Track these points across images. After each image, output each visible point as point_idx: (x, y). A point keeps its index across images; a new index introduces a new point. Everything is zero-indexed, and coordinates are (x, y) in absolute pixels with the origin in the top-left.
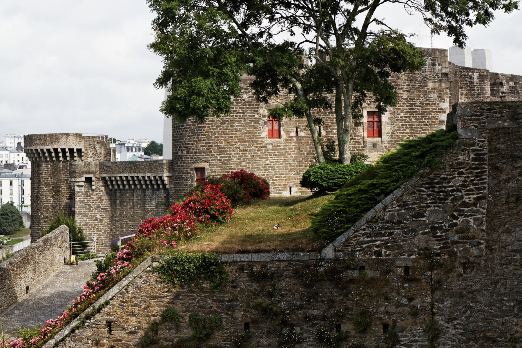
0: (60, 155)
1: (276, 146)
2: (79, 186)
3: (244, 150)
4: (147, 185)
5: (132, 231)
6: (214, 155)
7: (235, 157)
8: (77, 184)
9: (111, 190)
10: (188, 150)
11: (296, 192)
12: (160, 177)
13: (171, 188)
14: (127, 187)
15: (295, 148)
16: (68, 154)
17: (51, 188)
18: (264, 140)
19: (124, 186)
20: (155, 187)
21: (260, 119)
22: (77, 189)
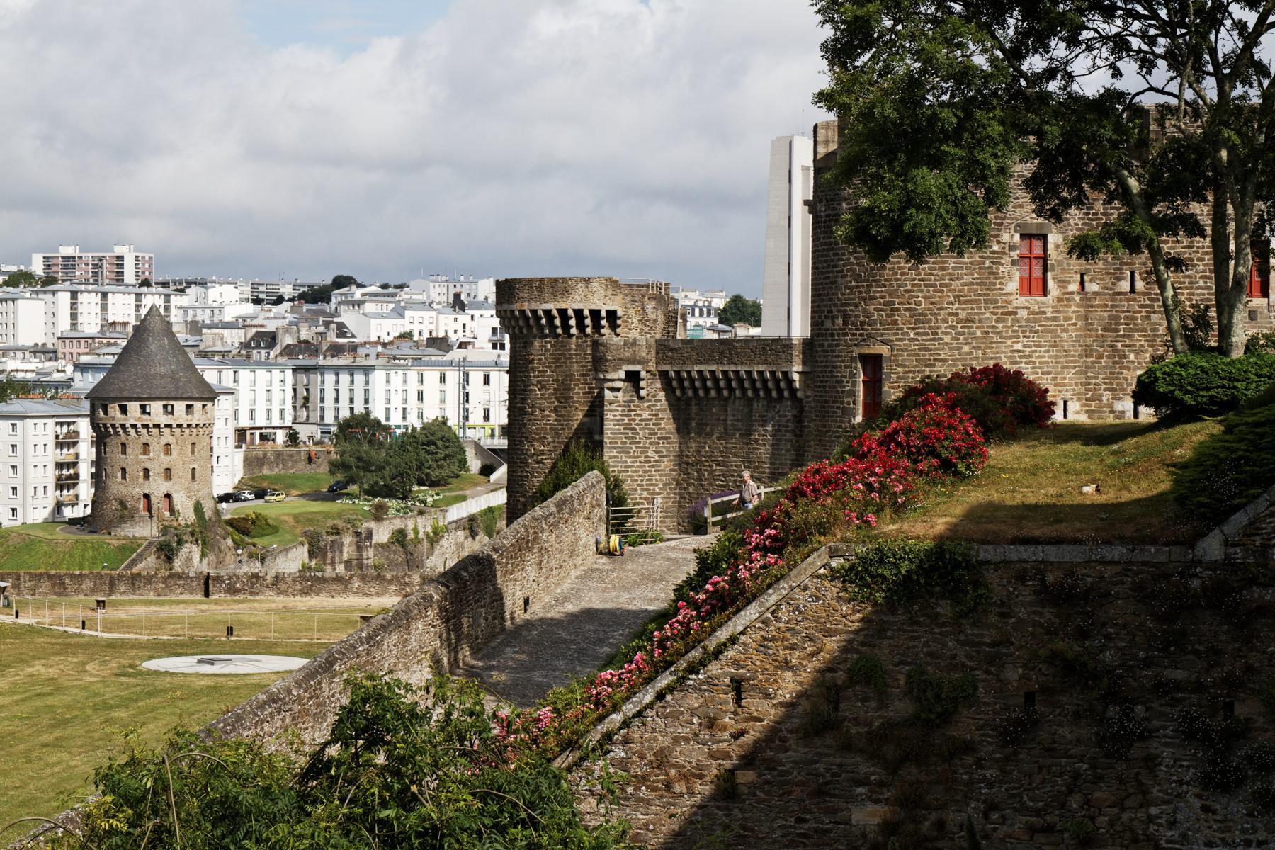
0: (573, 322)
1: (1038, 313)
2: (613, 389)
3: (967, 320)
4: (756, 391)
6: (902, 329)
7: (947, 334)
8: (609, 384)
9: (679, 399)
10: (846, 317)
11: (1078, 413)
12: (786, 374)
13: (807, 397)
14: (713, 393)
15: (1077, 318)
16: (588, 321)
17: (551, 391)
18: (1010, 298)
19: (707, 390)
20: (774, 394)
21: (1004, 253)
22: (608, 395)
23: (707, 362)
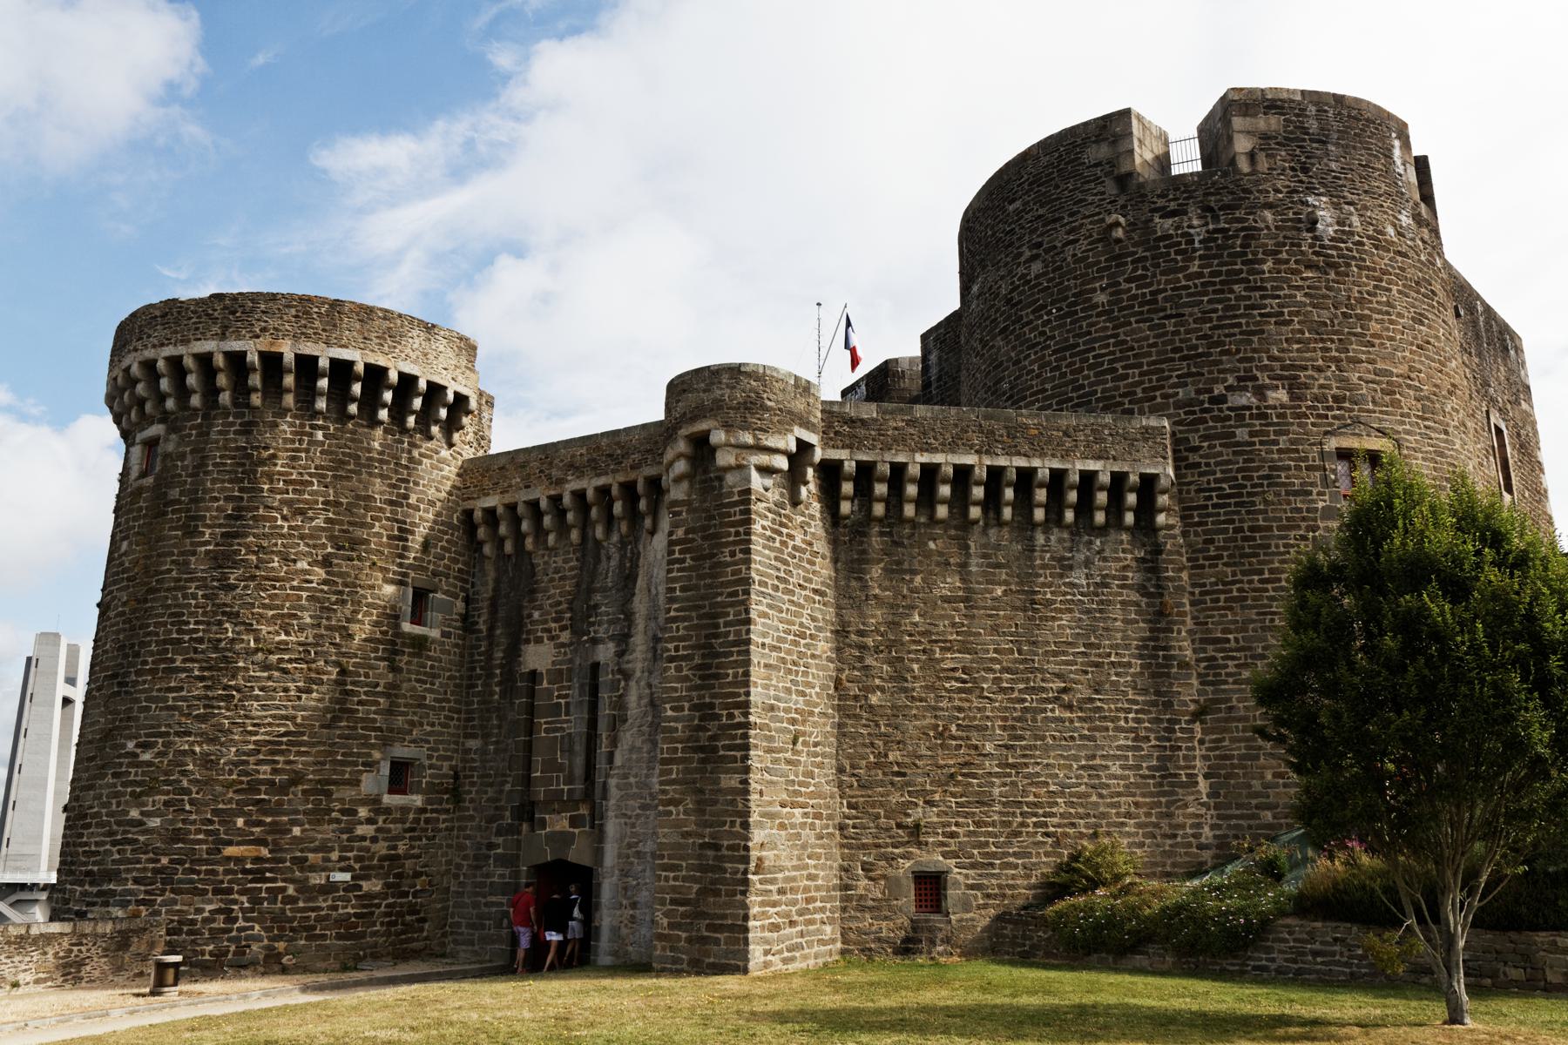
5: (960, 690)
8: (764, 459)
23: (952, 447)
